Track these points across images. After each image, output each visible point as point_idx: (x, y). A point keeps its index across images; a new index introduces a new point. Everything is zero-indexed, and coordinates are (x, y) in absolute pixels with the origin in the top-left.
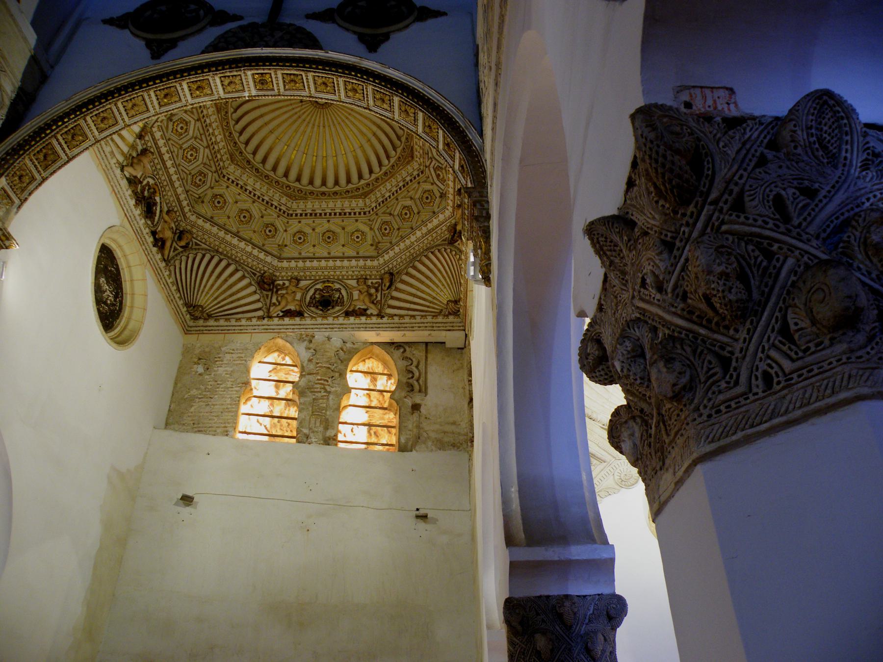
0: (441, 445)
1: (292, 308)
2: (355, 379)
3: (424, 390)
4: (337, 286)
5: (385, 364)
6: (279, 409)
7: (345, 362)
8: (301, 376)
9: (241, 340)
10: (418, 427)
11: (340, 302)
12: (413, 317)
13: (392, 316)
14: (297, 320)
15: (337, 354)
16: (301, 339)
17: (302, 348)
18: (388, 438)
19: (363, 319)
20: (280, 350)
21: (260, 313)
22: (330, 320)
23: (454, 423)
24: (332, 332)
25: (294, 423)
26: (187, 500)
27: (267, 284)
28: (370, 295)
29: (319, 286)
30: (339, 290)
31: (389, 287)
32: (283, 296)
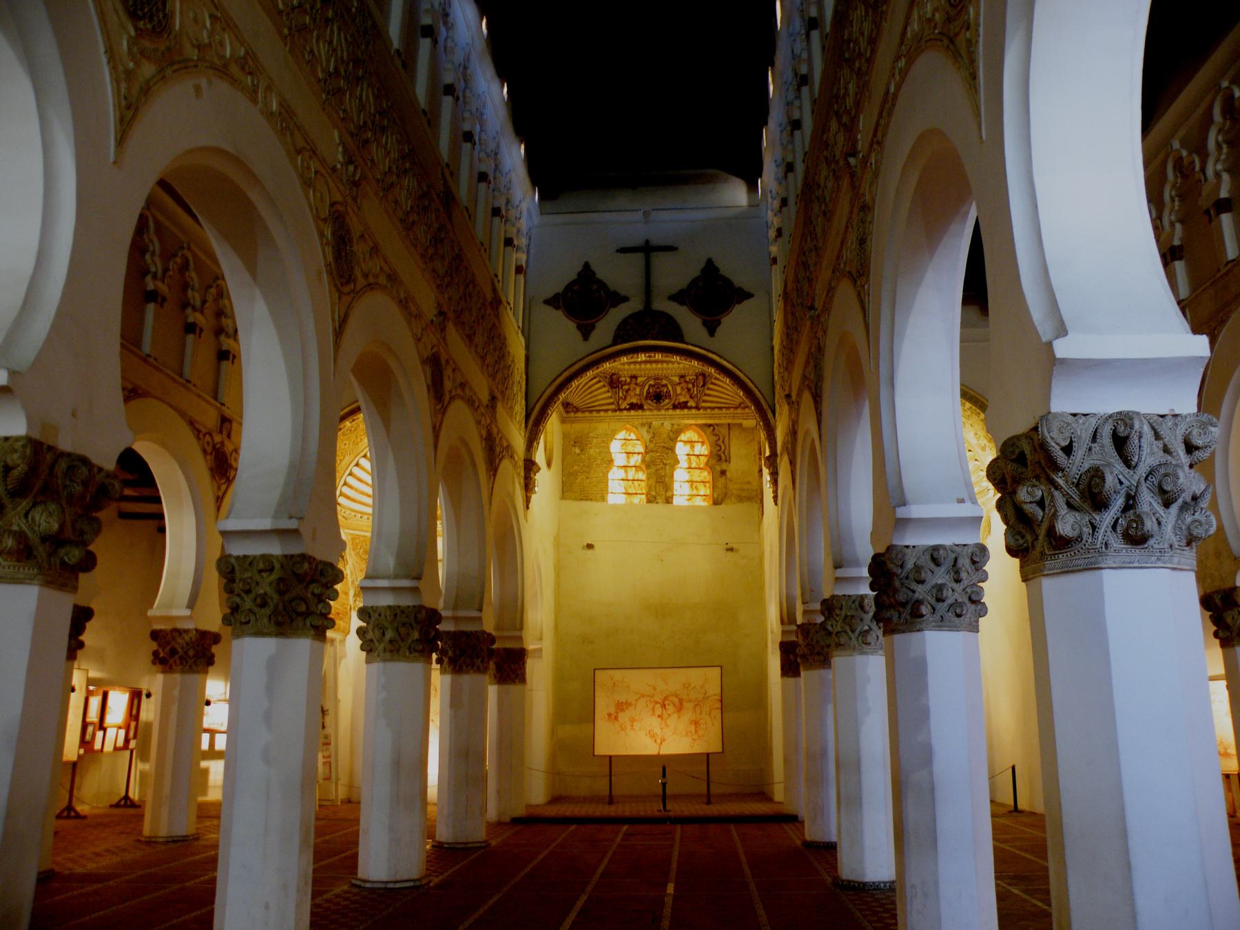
0: (741, 499)
1: (634, 401)
2: (681, 450)
3: (728, 461)
4: (664, 382)
5: (699, 435)
6: (632, 474)
7: (674, 440)
8: (646, 453)
9: (602, 427)
10: (726, 487)
11: (668, 395)
12: (720, 408)
13: (705, 408)
14: (640, 412)
15: (668, 436)
16: (643, 425)
17: (644, 431)
18: (705, 490)
19: (686, 411)
20: (627, 429)
21: (613, 407)
22: (663, 412)
23: (748, 483)
24: (664, 419)
25: (643, 484)
26: (590, 546)
27: (614, 382)
28: (689, 390)
29: (652, 382)
30: (665, 386)
31: (703, 386)
32: (627, 391)
